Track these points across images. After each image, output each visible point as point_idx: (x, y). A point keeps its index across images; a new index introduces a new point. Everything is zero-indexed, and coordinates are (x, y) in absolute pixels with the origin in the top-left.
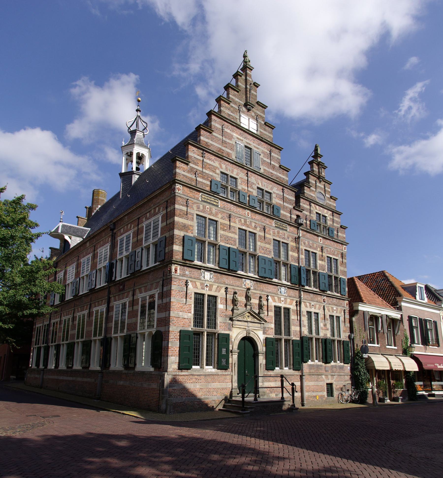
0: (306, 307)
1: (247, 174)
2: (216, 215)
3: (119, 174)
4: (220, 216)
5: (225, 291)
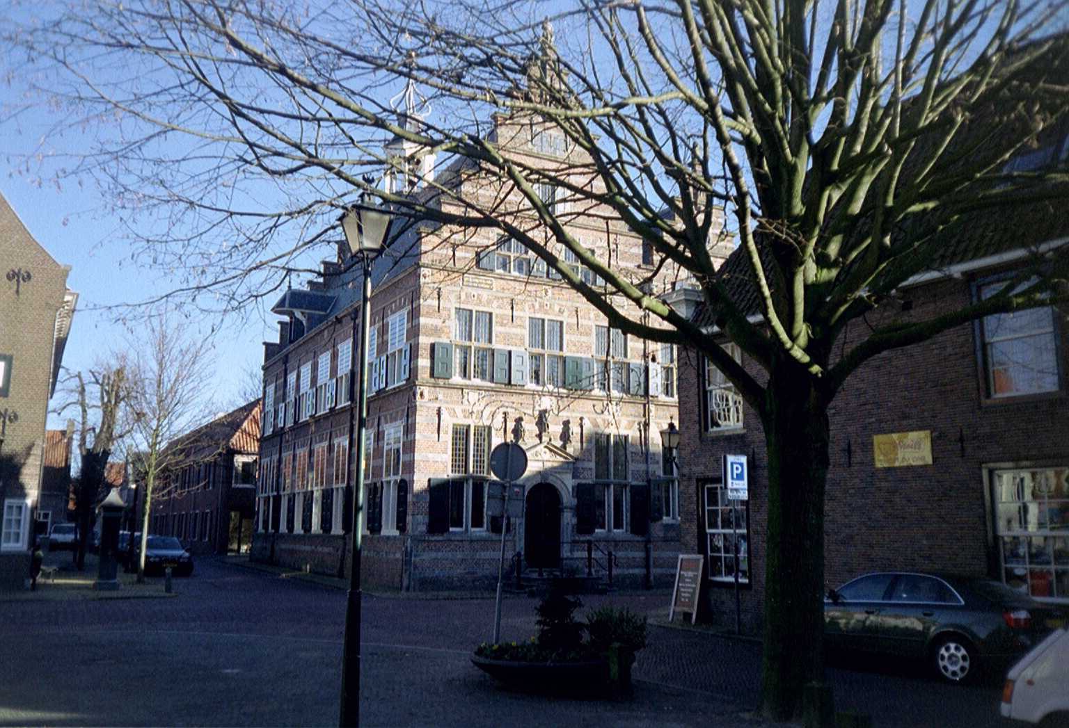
2: (489, 302)
4: (495, 304)
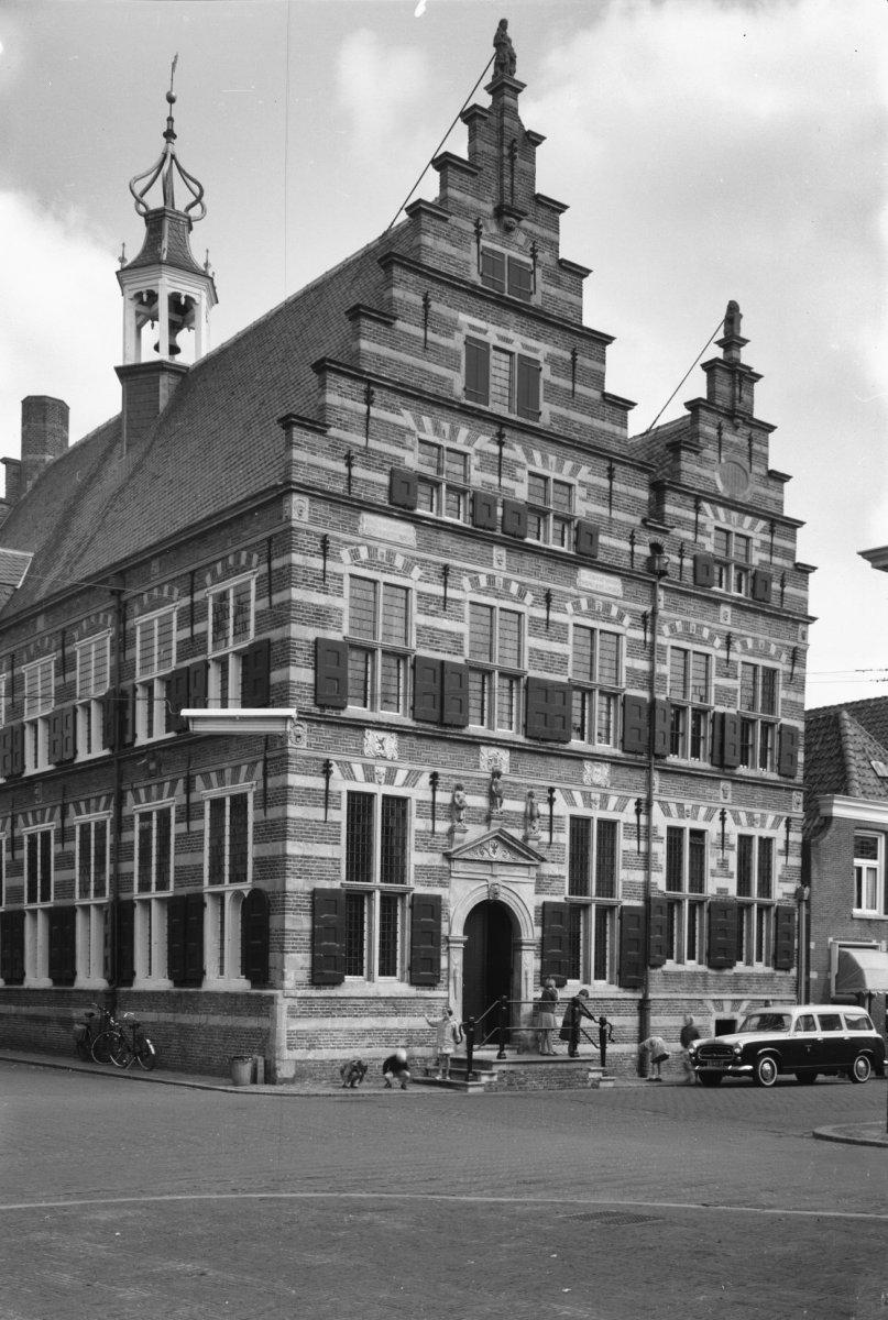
0: (667, 813)
3: (119, 370)
4: (417, 572)
5: (431, 783)
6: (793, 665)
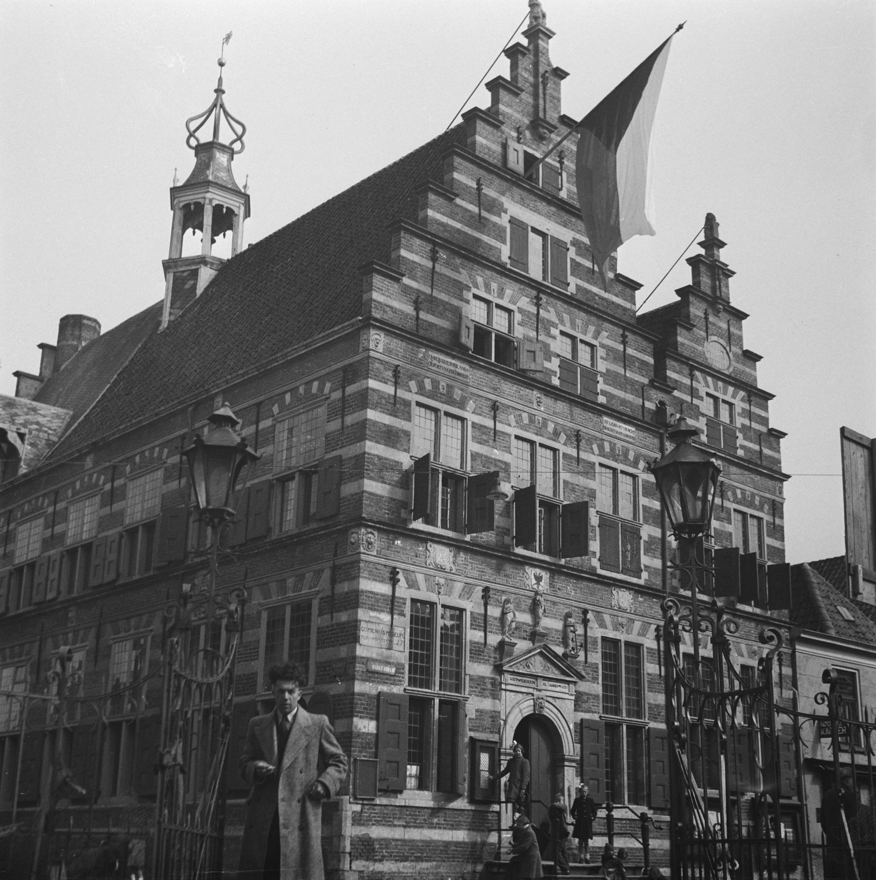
1: (538, 298)
4: (471, 405)
5: (483, 597)
6: (774, 515)
